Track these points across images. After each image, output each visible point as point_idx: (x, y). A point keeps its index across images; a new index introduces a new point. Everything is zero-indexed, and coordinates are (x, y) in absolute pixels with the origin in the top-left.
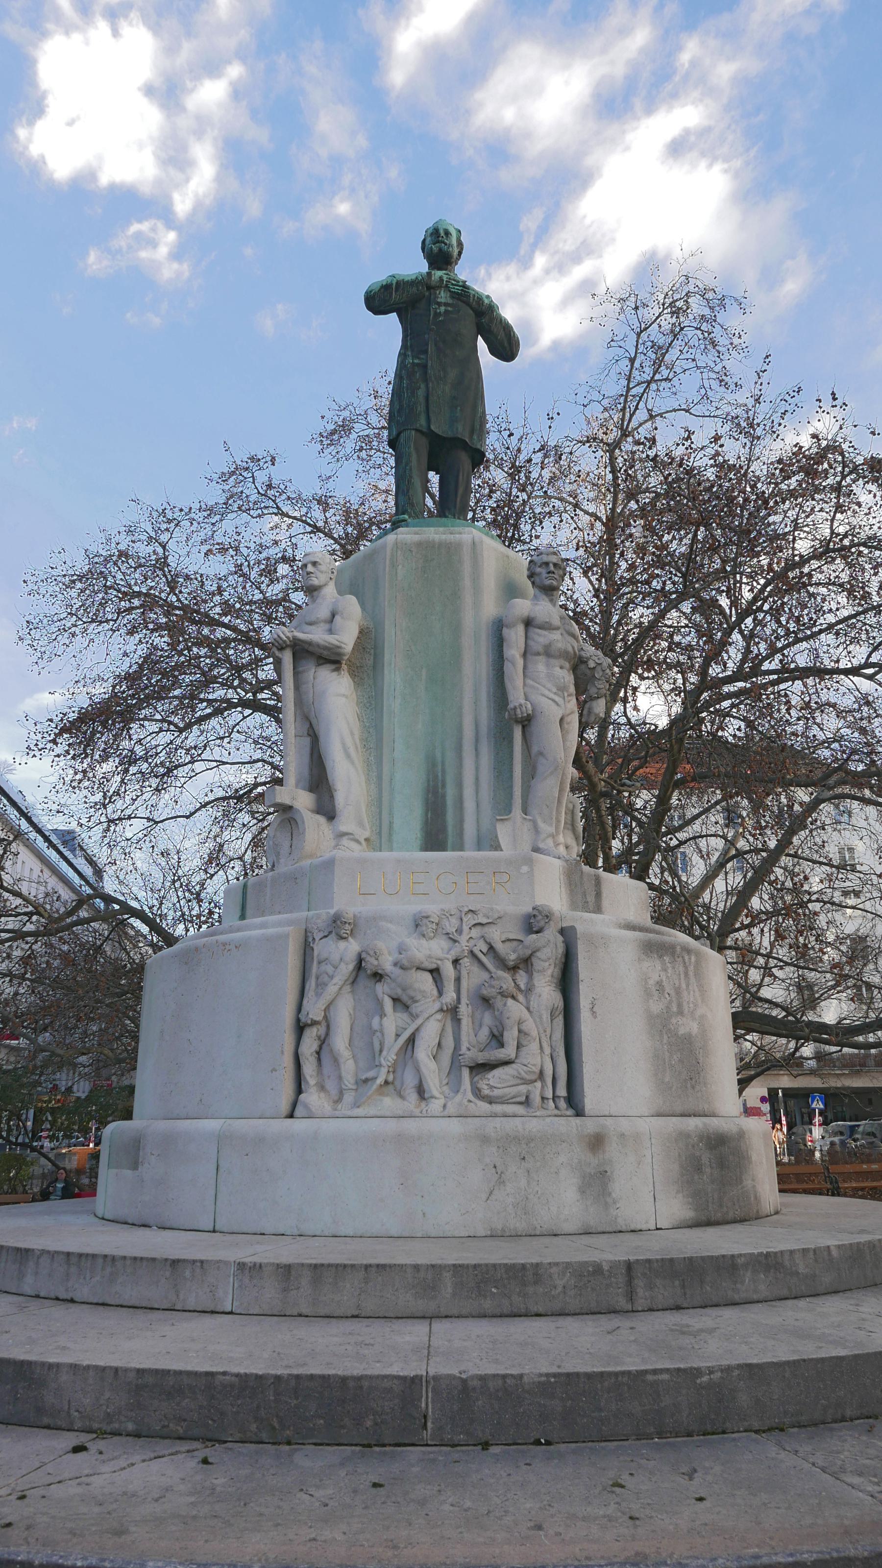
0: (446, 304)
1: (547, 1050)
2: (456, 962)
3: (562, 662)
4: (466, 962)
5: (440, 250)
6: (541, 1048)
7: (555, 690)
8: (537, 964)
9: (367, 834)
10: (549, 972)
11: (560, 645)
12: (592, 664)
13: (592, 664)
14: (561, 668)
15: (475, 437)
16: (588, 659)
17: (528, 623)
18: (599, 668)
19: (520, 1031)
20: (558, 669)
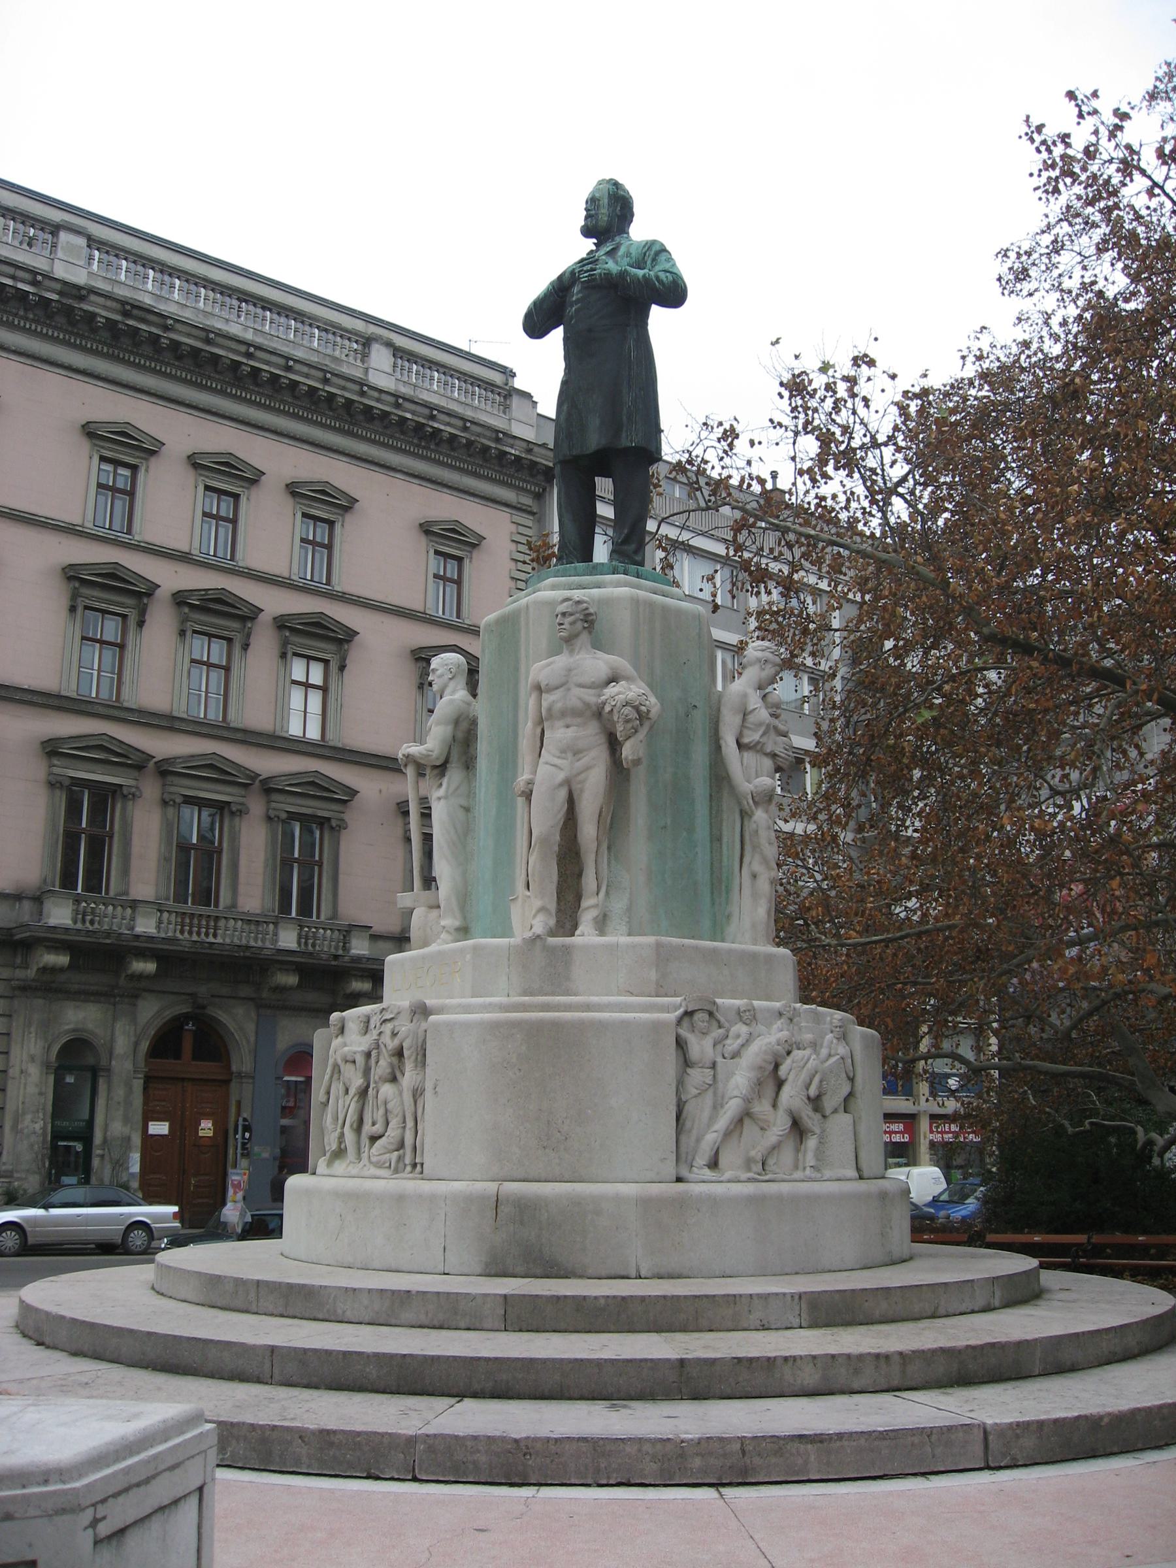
0: (577, 301)
1: (410, 1123)
2: (368, 1055)
3: (568, 720)
4: (374, 1053)
5: (609, 213)
6: (404, 1122)
7: (558, 754)
8: (406, 1053)
9: (457, 923)
10: (413, 1058)
11: (559, 705)
12: (607, 708)
13: (607, 708)
14: (568, 727)
15: (624, 435)
16: (604, 703)
17: (539, 689)
18: (615, 711)
19: (386, 1111)
20: (563, 730)
